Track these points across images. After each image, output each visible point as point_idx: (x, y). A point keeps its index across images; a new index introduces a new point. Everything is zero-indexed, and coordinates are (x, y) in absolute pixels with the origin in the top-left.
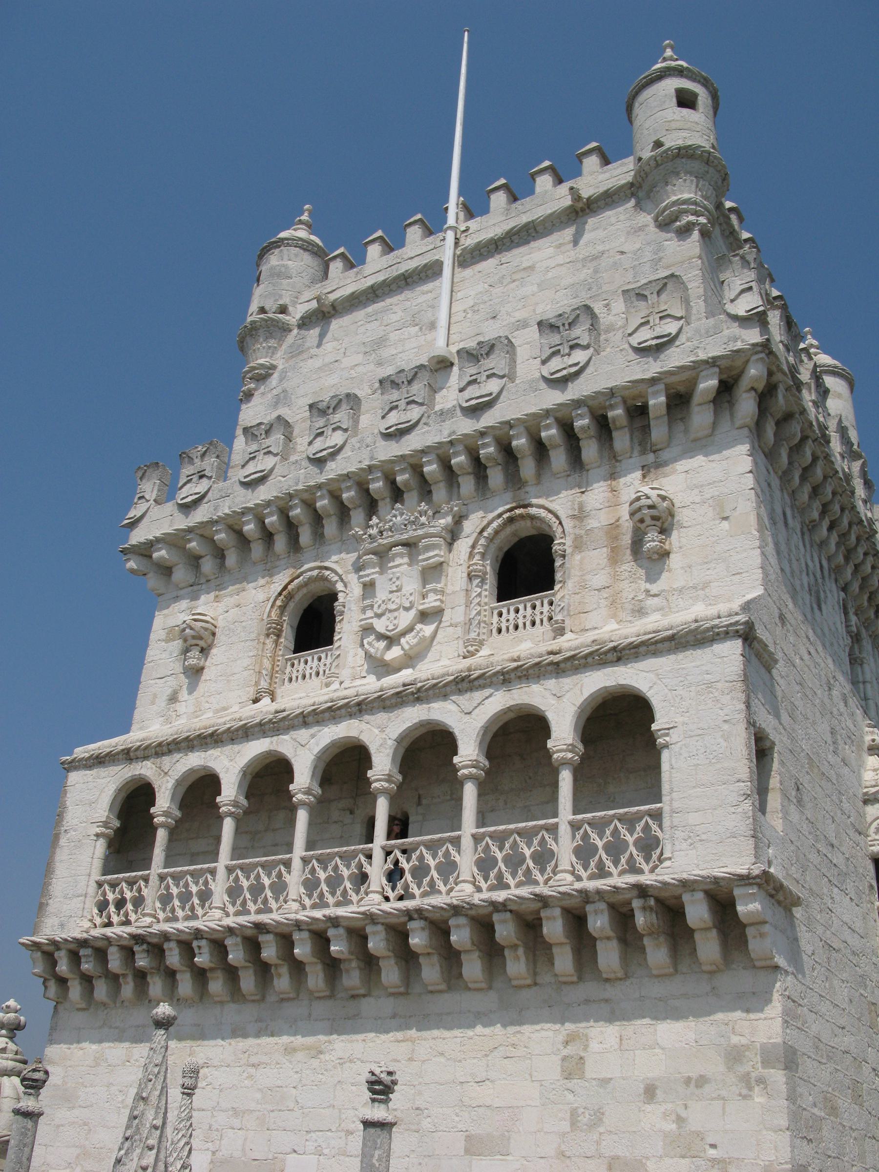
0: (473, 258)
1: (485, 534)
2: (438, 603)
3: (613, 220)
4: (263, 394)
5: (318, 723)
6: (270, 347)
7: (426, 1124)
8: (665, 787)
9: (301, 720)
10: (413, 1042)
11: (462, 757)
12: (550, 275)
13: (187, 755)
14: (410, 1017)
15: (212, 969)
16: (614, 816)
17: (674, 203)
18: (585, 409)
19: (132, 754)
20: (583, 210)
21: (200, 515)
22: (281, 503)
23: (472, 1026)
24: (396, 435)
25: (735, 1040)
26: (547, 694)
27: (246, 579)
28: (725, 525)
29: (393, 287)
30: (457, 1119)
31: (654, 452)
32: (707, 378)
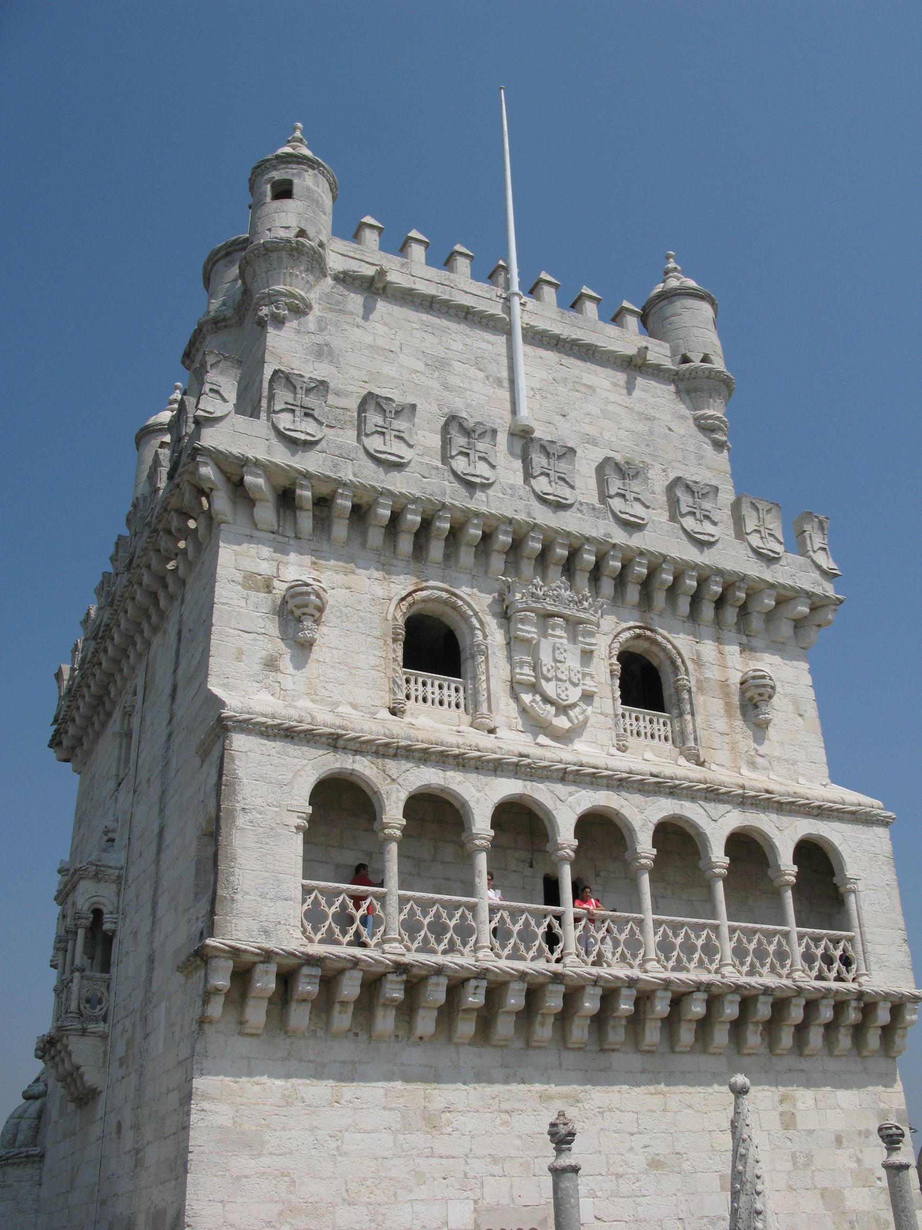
0: (533, 338)
3: (659, 393)
5: (575, 783)
6: (308, 282)
7: (686, 1166)
8: (855, 922)
9: (561, 775)
10: (664, 1095)
12: (611, 408)
14: (658, 1073)
19: (341, 743)
23: (709, 1084)
25: (882, 1105)
28: (799, 718)
29: (452, 311)
30: (710, 1161)
31: (747, 636)
32: (803, 605)
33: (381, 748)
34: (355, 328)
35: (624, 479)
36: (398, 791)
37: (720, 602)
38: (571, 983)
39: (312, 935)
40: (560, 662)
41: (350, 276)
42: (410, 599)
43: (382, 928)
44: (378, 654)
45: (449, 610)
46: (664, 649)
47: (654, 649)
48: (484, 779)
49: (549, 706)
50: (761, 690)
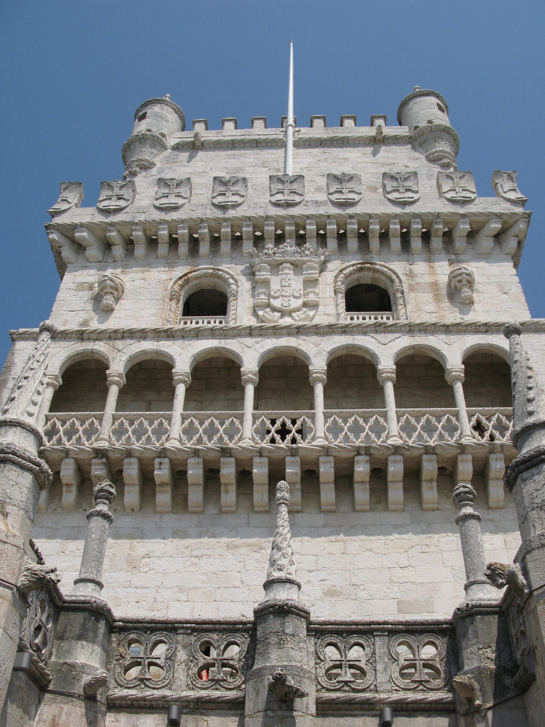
1: (344, 272)
4: (145, 177)
5: (261, 335)
6: (152, 153)
7: (362, 594)
9: (248, 331)
11: (385, 366)
12: (359, 165)
13: (139, 342)
14: (339, 526)
15: (163, 484)
16: (497, 410)
17: (441, 151)
19: (85, 335)
20: (379, 141)
22: (192, 223)
23: (390, 534)
24: (283, 206)
26: (441, 342)
27: (150, 266)
28: (504, 295)
29: (247, 145)
30: (389, 591)
31: (455, 254)
32: (495, 223)
33: (112, 334)
35: (341, 183)
36: (122, 356)
37: (426, 237)
40: (285, 286)
41: (181, 145)
42: (186, 278)
44: (158, 307)
46: (383, 273)
47: (377, 275)
48: (187, 342)
49: (276, 313)
50: (459, 278)
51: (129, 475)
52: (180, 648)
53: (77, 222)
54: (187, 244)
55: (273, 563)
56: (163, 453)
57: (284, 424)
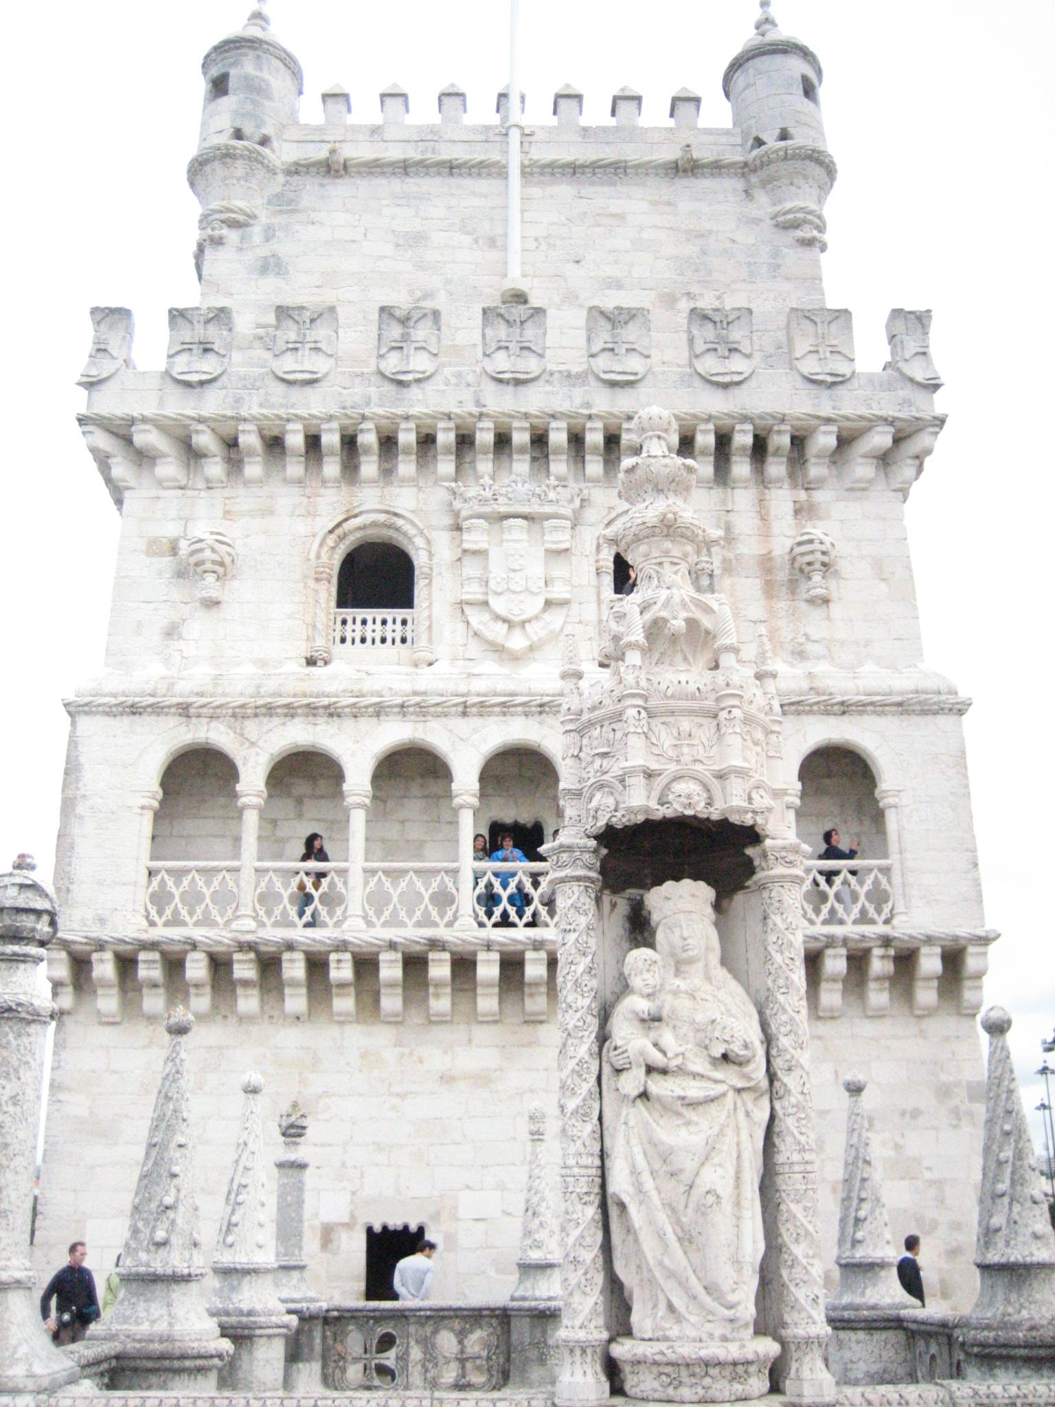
2: (568, 596)
9: (460, 709)
13: (284, 724)
17: (801, 209)
18: (749, 427)
19: (192, 711)
21: (213, 404)
25: (944, 1077)
28: (883, 586)
31: (807, 489)
34: (311, 227)
36: (257, 754)
38: (455, 949)
39: (156, 918)
40: (514, 571)
41: (304, 166)
42: (339, 531)
43: (234, 906)
45: (394, 534)
50: (808, 558)
51: (292, 979)
52: (412, 1343)
53: (135, 415)
54: (338, 459)
55: (528, 1233)
56: (342, 946)
57: (520, 888)
